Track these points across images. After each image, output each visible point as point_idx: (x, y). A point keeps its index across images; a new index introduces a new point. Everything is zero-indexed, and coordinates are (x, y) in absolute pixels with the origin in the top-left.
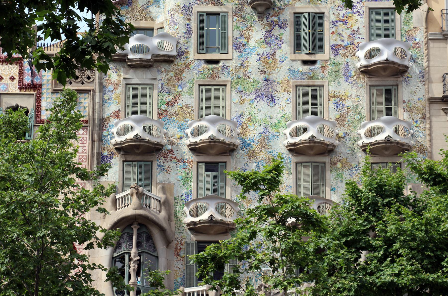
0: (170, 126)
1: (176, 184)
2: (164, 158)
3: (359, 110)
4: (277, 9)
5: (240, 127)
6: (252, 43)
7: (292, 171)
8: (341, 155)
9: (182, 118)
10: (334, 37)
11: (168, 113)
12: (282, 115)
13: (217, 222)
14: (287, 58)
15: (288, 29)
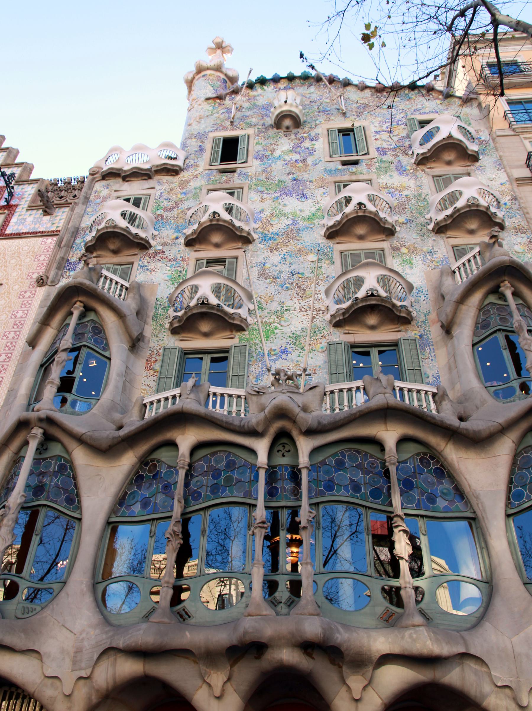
0: (165, 229)
1: (162, 285)
2: (150, 258)
3: (423, 197)
4: (306, 129)
5: (259, 223)
6: (277, 153)
7: (334, 260)
8: (406, 241)
9: (181, 220)
10: (379, 142)
11: (165, 217)
12: (318, 208)
13: (212, 307)
14: (321, 161)
15: (321, 140)
